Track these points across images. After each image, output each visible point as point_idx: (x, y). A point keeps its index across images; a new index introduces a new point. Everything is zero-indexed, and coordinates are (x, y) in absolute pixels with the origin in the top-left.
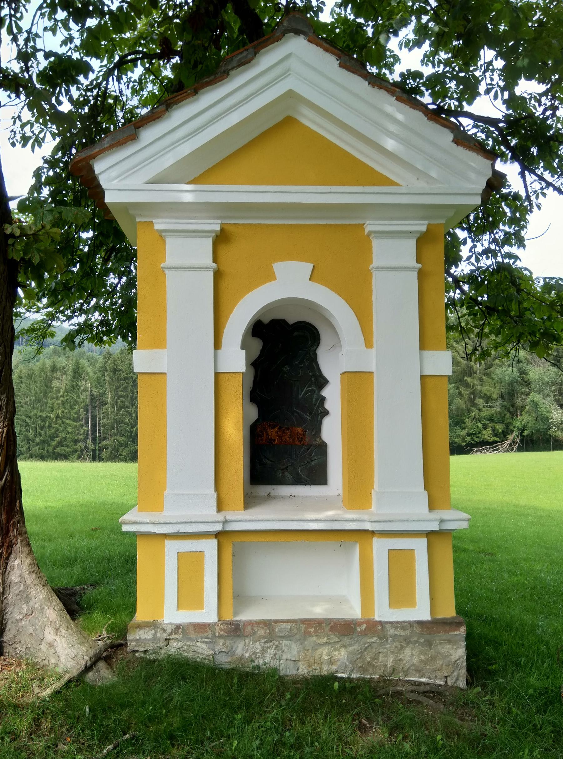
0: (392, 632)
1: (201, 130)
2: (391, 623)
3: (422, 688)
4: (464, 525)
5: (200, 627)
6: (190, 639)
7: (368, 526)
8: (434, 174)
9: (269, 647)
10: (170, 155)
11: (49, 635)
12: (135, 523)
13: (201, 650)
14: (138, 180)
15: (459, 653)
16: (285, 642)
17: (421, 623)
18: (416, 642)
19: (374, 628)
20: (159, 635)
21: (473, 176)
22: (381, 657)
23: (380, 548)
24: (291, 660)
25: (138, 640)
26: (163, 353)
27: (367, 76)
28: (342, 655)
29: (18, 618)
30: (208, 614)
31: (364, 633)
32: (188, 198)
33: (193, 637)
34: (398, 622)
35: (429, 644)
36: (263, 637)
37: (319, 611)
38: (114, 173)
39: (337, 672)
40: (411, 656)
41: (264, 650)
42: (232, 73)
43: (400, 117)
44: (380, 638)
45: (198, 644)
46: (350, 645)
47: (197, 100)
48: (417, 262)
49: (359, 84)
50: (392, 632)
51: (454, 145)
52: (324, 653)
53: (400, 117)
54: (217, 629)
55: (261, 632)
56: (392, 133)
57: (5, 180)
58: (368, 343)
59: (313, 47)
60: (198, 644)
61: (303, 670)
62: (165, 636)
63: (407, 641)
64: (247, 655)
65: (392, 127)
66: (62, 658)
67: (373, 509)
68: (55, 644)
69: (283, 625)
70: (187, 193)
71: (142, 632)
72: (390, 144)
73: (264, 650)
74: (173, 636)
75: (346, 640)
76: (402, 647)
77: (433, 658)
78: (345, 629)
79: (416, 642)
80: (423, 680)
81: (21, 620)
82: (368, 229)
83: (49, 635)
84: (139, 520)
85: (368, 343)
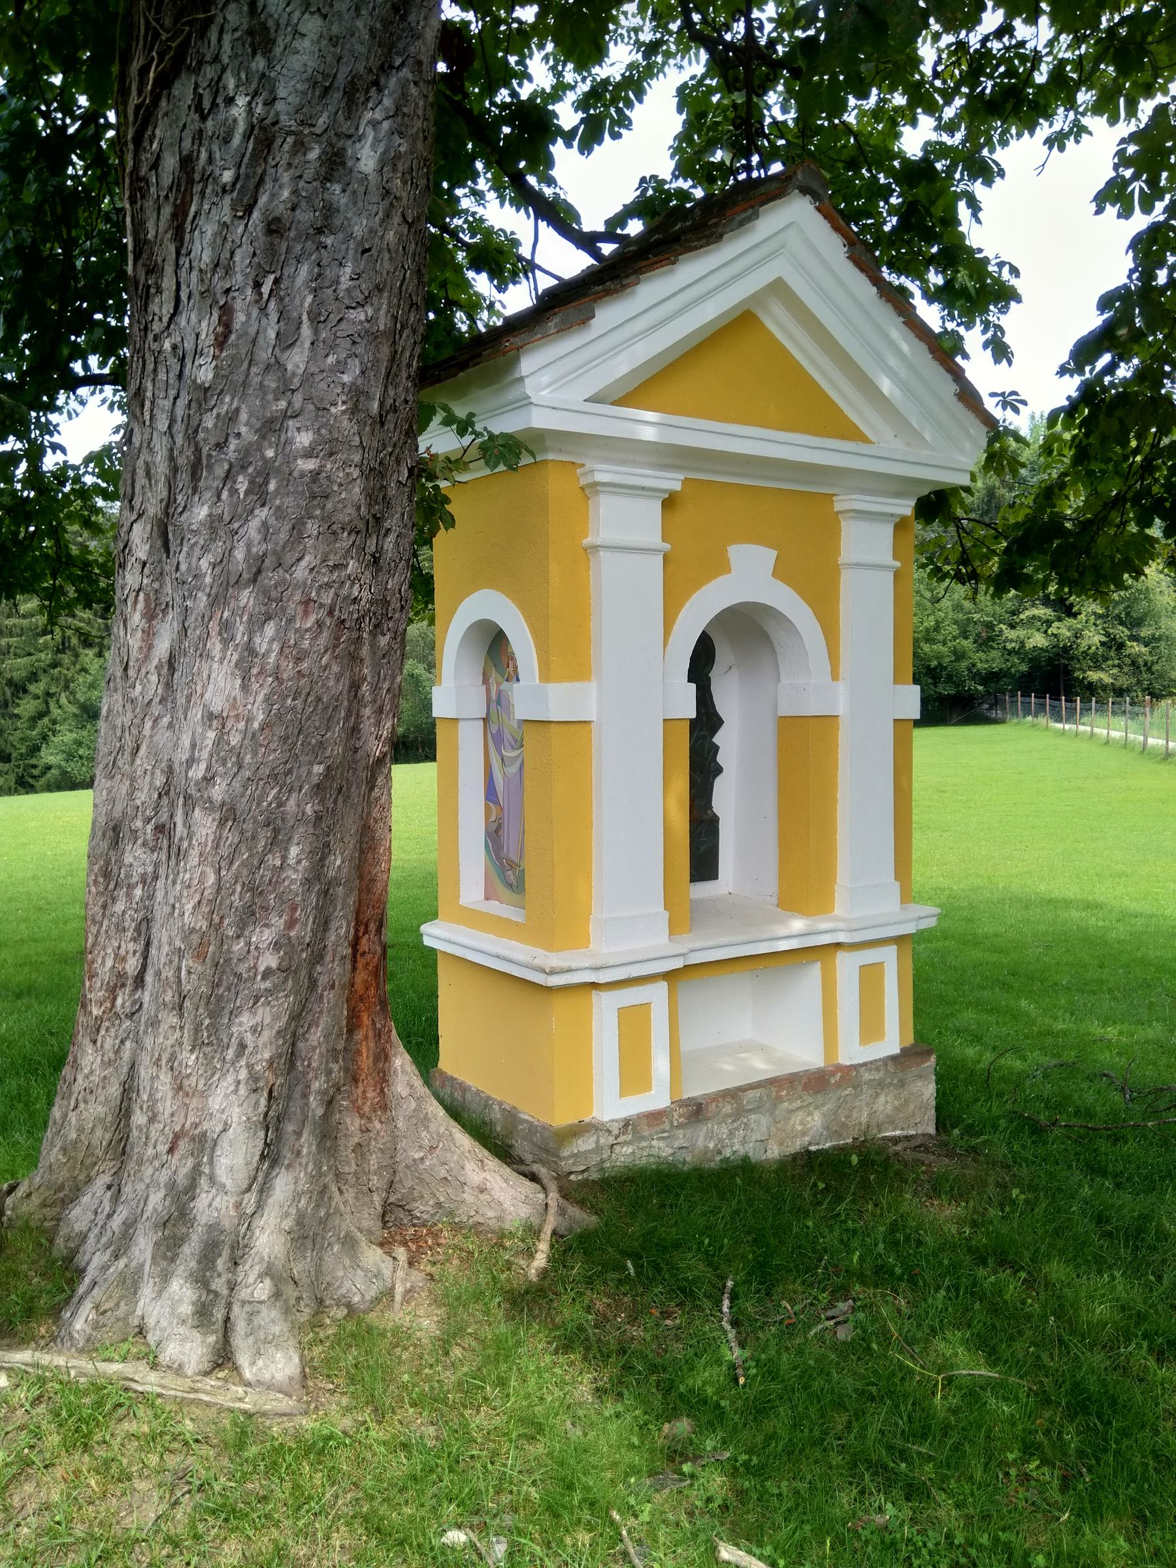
0: (867, 1076)
1: (641, 324)
2: (865, 1064)
3: (914, 1143)
4: (933, 922)
5: (655, 1117)
6: (643, 1138)
7: (842, 938)
8: (927, 437)
9: (737, 1129)
10: (622, 357)
11: (473, 1174)
12: (569, 970)
13: (661, 1149)
14: (576, 394)
15: (928, 1090)
16: (753, 1117)
17: (893, 1058)
18: (891, 1084)
19: (849, 1075)
20: (602, 1141)
21: (968, 446)
22: (855, 1114)
23: (847, 966)
24: (766, 1139)
25: (574, 1155)
26: (591, 688)
27: (877, 281)
28: (816, 1120)
29: (417, 1156)
30: (658, 1098)
31: (838, 1085)
32: (649, 434)
33: (646, 1133)
34: (871, 1062)
35: (902, 1084)
36: (730, 1116)
37: (761, 1068)
38: (545, 378)
39: (810, 1144)
40: (885, 1104)
41: (731, 1134)
42: (725, 237)
43: (905, 347)
44: (855, 1088)
45: (655, 1143)
46: (823, 1105)
47: (672, 271)
48: (895, 558)
49: (865, 289)
50: (867, 1076)
51: (955, 399)
52: (796, 1122)
53: (905, 347)
54: (676, 1115)
55: (728, 1109)
56: (890, 368)
57: (1085, 333)
58: (835, 676)
59: (819, 217)
60: (655, 1143)
61: (774, 1152)
62: (611, 1140)
63: (880, 1085)
64: (711, 1146)
65: (893, 361)
66: (507, 1204)
67: (837, 911)
68: (488, 1186)
69: (752, 1094)
70: (646, 425)
71: (580, 1142)
72: (886, 385)
73: (731, 1134)
74: (621, 1139)
75: (820, 1098)
76: (877, 1094)
77: (907, 1102)
78: (816, 1082)
79: (891, 1084)
80: (898, 1133)
81: (422, 1159)
82: (838, 507)
83: (473, 1174)
84: (573, 965)
85: (835, 676)
